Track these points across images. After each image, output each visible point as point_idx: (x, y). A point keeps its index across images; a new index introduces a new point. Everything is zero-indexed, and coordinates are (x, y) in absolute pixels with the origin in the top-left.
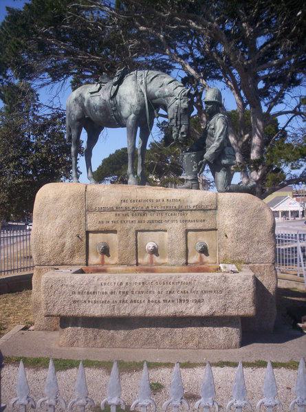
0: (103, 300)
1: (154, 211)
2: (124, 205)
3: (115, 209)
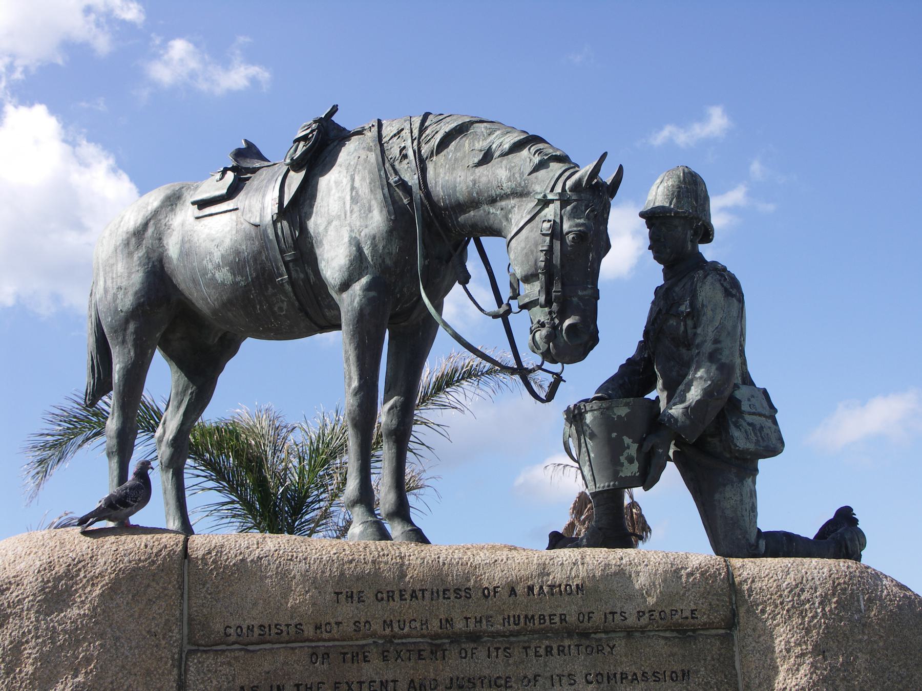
1: (475, 637)
2: (347, 611)
3: (309, 631)
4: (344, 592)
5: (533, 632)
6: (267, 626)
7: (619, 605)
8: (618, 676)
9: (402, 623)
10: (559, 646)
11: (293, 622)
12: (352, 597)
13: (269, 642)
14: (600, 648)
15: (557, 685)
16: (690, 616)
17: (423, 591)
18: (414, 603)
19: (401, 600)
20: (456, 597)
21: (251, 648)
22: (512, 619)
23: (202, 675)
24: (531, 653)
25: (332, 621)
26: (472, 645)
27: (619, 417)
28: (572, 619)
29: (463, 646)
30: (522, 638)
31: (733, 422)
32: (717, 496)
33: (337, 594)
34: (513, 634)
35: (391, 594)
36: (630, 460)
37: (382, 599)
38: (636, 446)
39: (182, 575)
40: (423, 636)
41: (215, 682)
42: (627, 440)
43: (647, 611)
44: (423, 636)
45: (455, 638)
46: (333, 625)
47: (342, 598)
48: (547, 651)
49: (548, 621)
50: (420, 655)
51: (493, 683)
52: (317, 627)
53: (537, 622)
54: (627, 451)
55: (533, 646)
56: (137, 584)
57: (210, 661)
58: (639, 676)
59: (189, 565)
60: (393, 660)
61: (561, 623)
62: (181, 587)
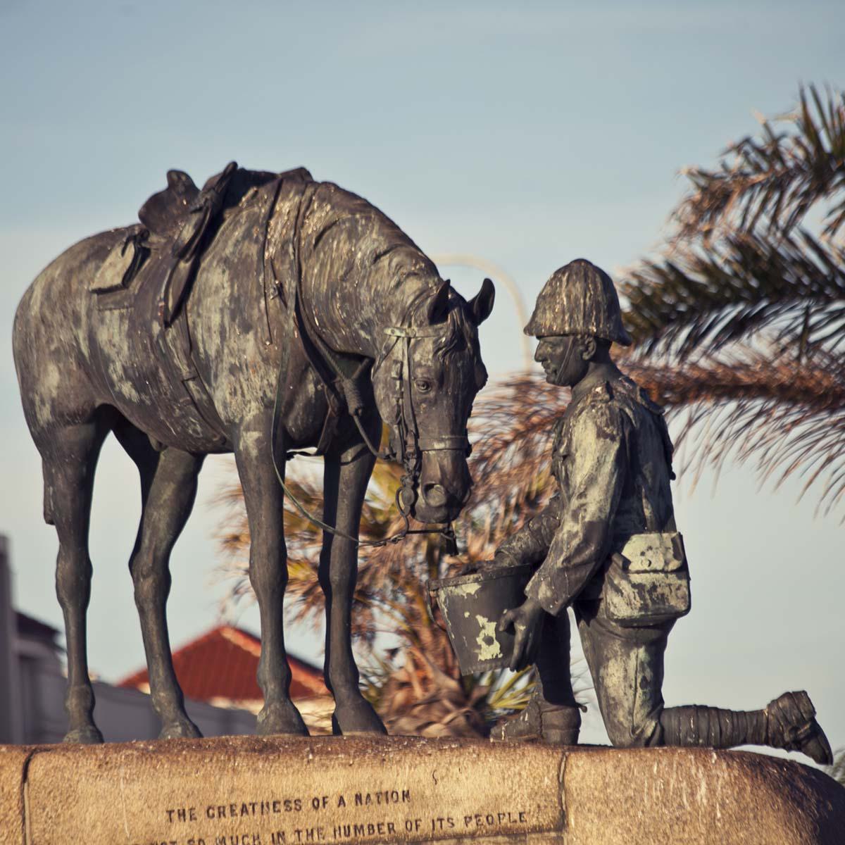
4: (176, 811)
7: (446, 811)
9: (235, 840)
16: (518, 820)
17: (253, 805)
18: (245, 817)
19: (232, 815)
20: (286, 810)
27: (469, 594)
28: (399, 827)
33: (170, 812)
35: (222, 810)
36: (489, 641)
38: (493, 625)
39: (22, 800)
42: (481, 620)
47: (175, 816)
54: (483, 631)
59: (28, 790)
61: (390, 833)
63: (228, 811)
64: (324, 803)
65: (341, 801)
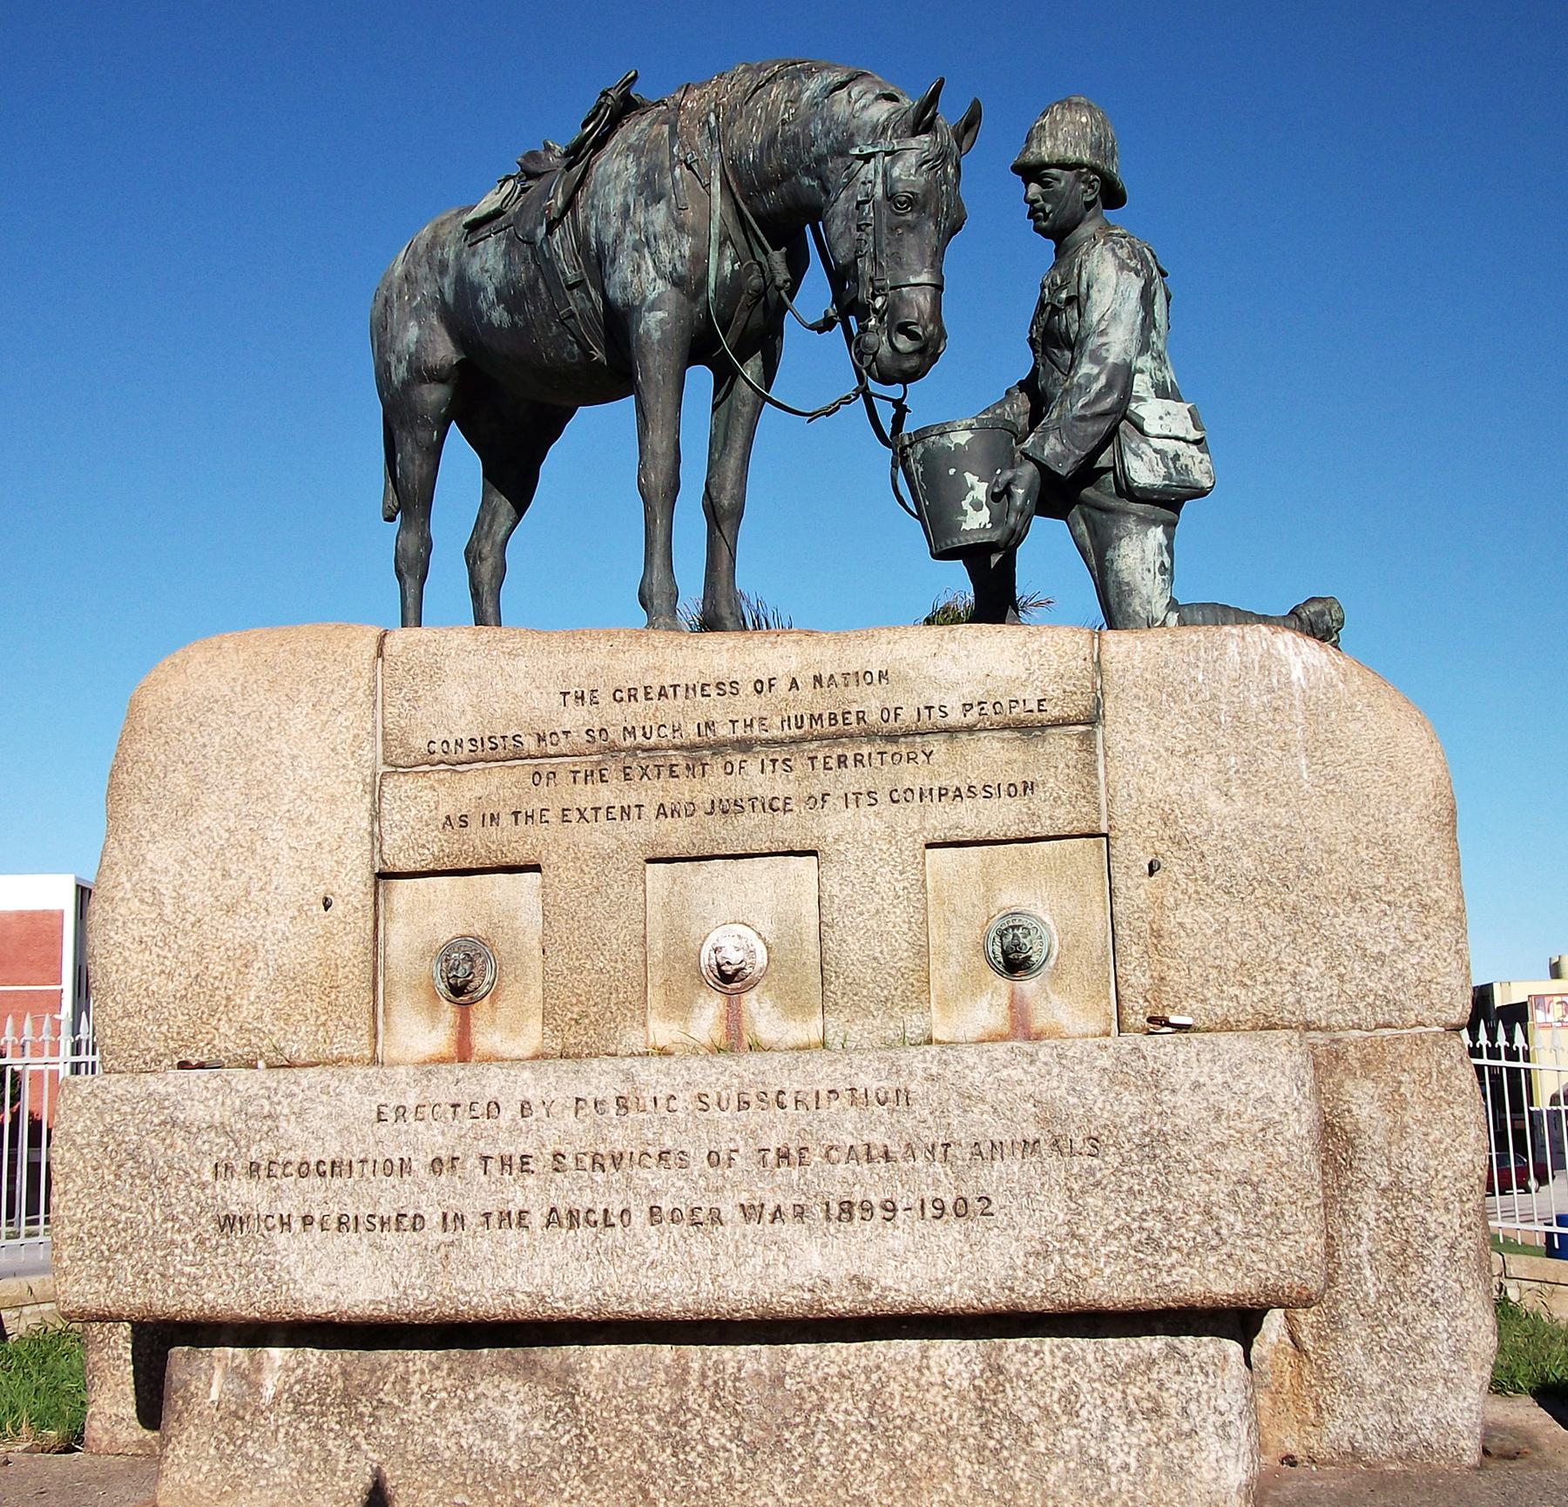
0: (386, 1210)
1: (745, 746)
2: (575, 718)
4: (573, 692)
5: (821, 738)
6: (478, 739)
7: (936, 697)
8: (936, 792)
10: (855, 755)
11: (510, 734)
12: (582, 698)
13: (482, 760)
14: (912, 756)
15: (852, 806)
16: (1036, 709)
17: (675, 687)
19: (647, 699)
21: (459, 768)
22: (793, 721)
23: (399, 803)
24: (819, 764)
25: (558, 731)
26: (740, 757)
28: (873, 718)
29: (728, 758)
30: (806, 746)
31: (1130, 449)
32: (1109, 554)
33: (565, 694)
34: (794, 741)
35: (633, 692)
36: (977, 506)
37: (622, 699)
40: (676, 748)
41: (414, 811)
42: (971, 478)
43: (975, 703)
44: (676, 748)
45: (718, 747)
46: (561, 735)
48: (839, 762)
49: (840, 721)
50: (672, 771)
51: (767, 806)
52: (541, 739)
53: (826, 723)
54: (971, 493)
55: (820, 757)
56: (319, 689)
57: (408, 785)
58: (964, 790)
60: (637, 779)
62: (373, 692)
63: (641, 694)
64: (771, 686)
65: (794, 683)
